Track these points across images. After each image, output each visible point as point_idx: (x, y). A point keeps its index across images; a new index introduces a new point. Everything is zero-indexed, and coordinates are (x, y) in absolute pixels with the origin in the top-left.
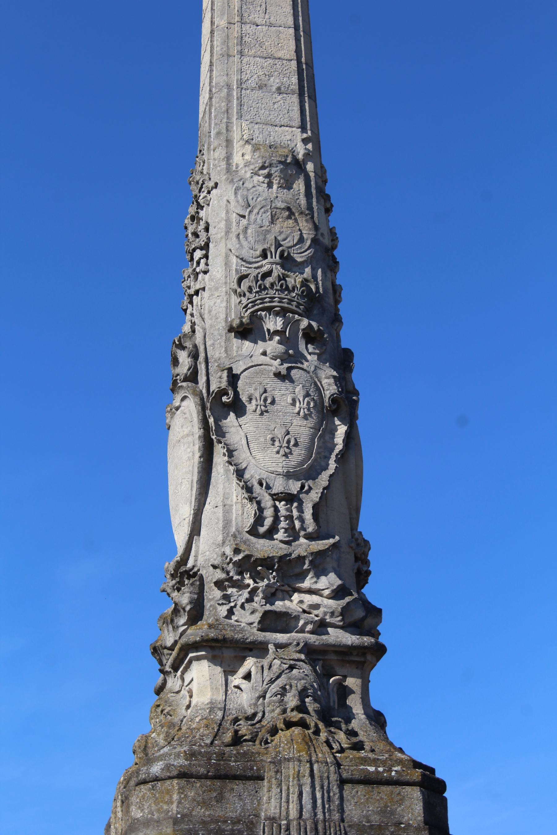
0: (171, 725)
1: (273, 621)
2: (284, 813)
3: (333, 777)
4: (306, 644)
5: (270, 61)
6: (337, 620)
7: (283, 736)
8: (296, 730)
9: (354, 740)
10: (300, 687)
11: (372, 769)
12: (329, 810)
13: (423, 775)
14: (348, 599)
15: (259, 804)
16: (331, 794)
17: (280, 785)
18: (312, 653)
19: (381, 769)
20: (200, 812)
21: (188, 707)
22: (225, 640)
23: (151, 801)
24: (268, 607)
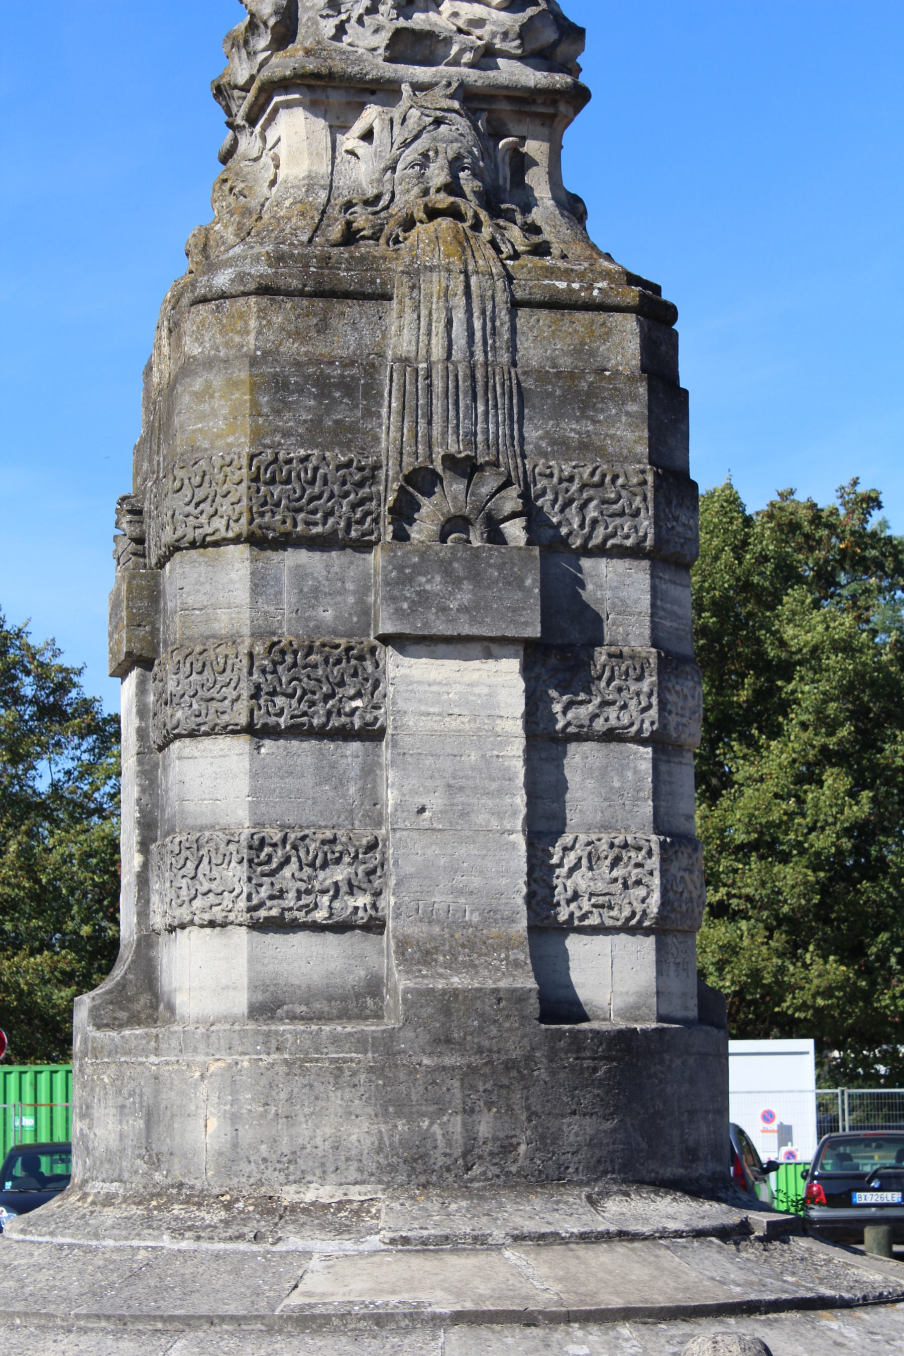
0: (246, 212)
1: (411, 46)
2: (422, 352)
3: (502, 297)
4: (462, 85)
6: (512, 46)
7: (423, 231)
8: (444, 223)
9: (536, 239)
10: (451, 155)
11: (562, 285)
12: (494, 348)
13: (642, 296)
14: (531, 11)
15: (384, 337)
16: (498, 324)
17: (417, 308)
18: (471, 99)
19: (576, 286)
21: (273, 183)
22: (331, 75)
23: (216, 329)
24: (402, 23)
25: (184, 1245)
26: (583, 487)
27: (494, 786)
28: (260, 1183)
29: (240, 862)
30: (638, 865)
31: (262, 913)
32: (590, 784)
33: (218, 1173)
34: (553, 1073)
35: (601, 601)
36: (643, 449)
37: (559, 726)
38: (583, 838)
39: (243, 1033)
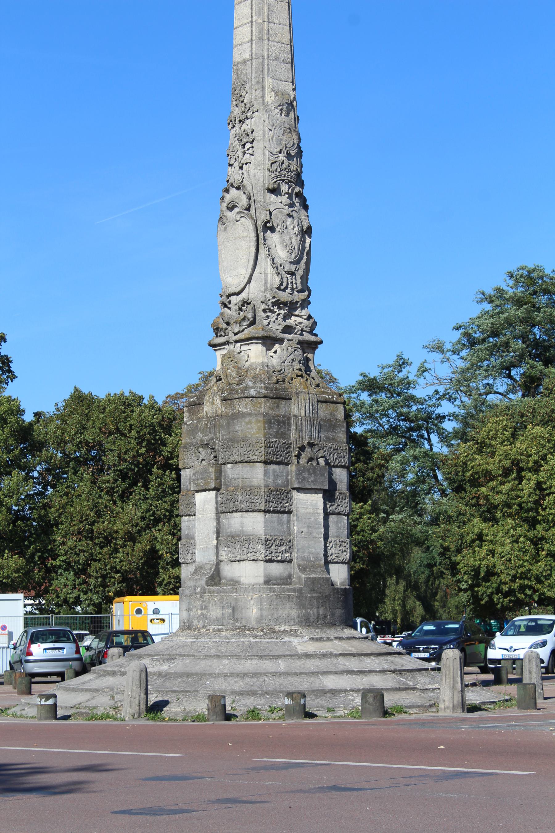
3: (316, 400)
5: (280, 44)
11: (327, 397)
20: (271, 412)
25: (257, 640)
26: (334, 449)
27: (317, 526)
28: (269, 625)
29: (262, 545)
30: (345, 547)
31: (268, 558)
32: (334, 526)
33: (256, 623)
34: (334, 598)
35: (336, 479)
36: (345, 440)
37: (328, 511)
38: (333, 540)
39: (263, 588)
